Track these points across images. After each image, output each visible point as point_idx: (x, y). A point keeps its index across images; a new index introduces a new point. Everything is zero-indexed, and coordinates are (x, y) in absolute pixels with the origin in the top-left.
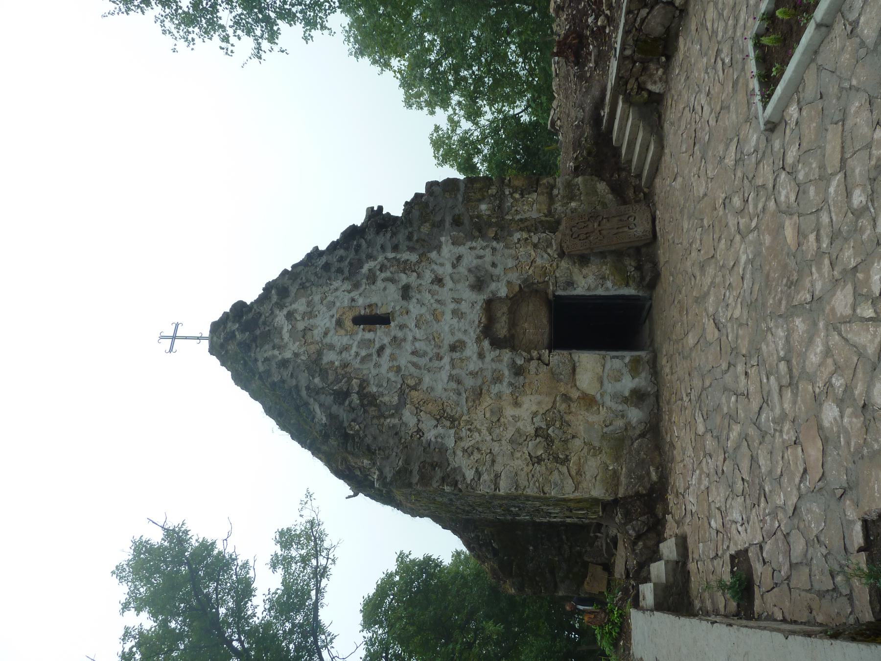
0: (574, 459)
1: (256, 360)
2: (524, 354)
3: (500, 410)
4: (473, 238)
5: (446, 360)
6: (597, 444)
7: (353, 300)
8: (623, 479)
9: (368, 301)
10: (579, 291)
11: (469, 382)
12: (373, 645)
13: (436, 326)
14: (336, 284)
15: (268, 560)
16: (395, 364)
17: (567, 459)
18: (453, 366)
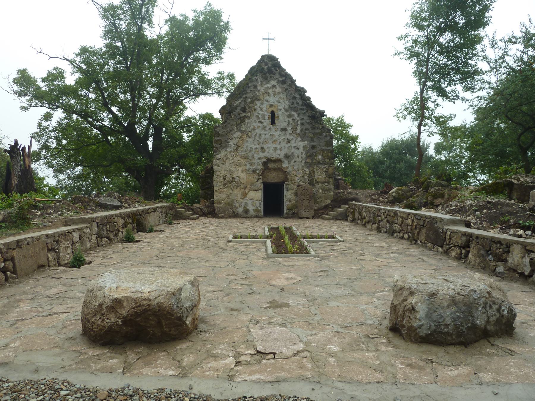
0: (225, 190)
1: (256, 76)
2: (260, 173)
3: (240, 166)
4: (306, 153)
5: (258, 146)
6: (230, 197)
7: (281, 110)
8: (219, 205)
9: (280, 116)
10: (285, 192)
11: (250, 155)
12: (194, 119)
13: (270, 142)
14: (287, 103)
15: (222, 70)
16: (256, 128)
17: (225, 188)
18: (256, 149)
